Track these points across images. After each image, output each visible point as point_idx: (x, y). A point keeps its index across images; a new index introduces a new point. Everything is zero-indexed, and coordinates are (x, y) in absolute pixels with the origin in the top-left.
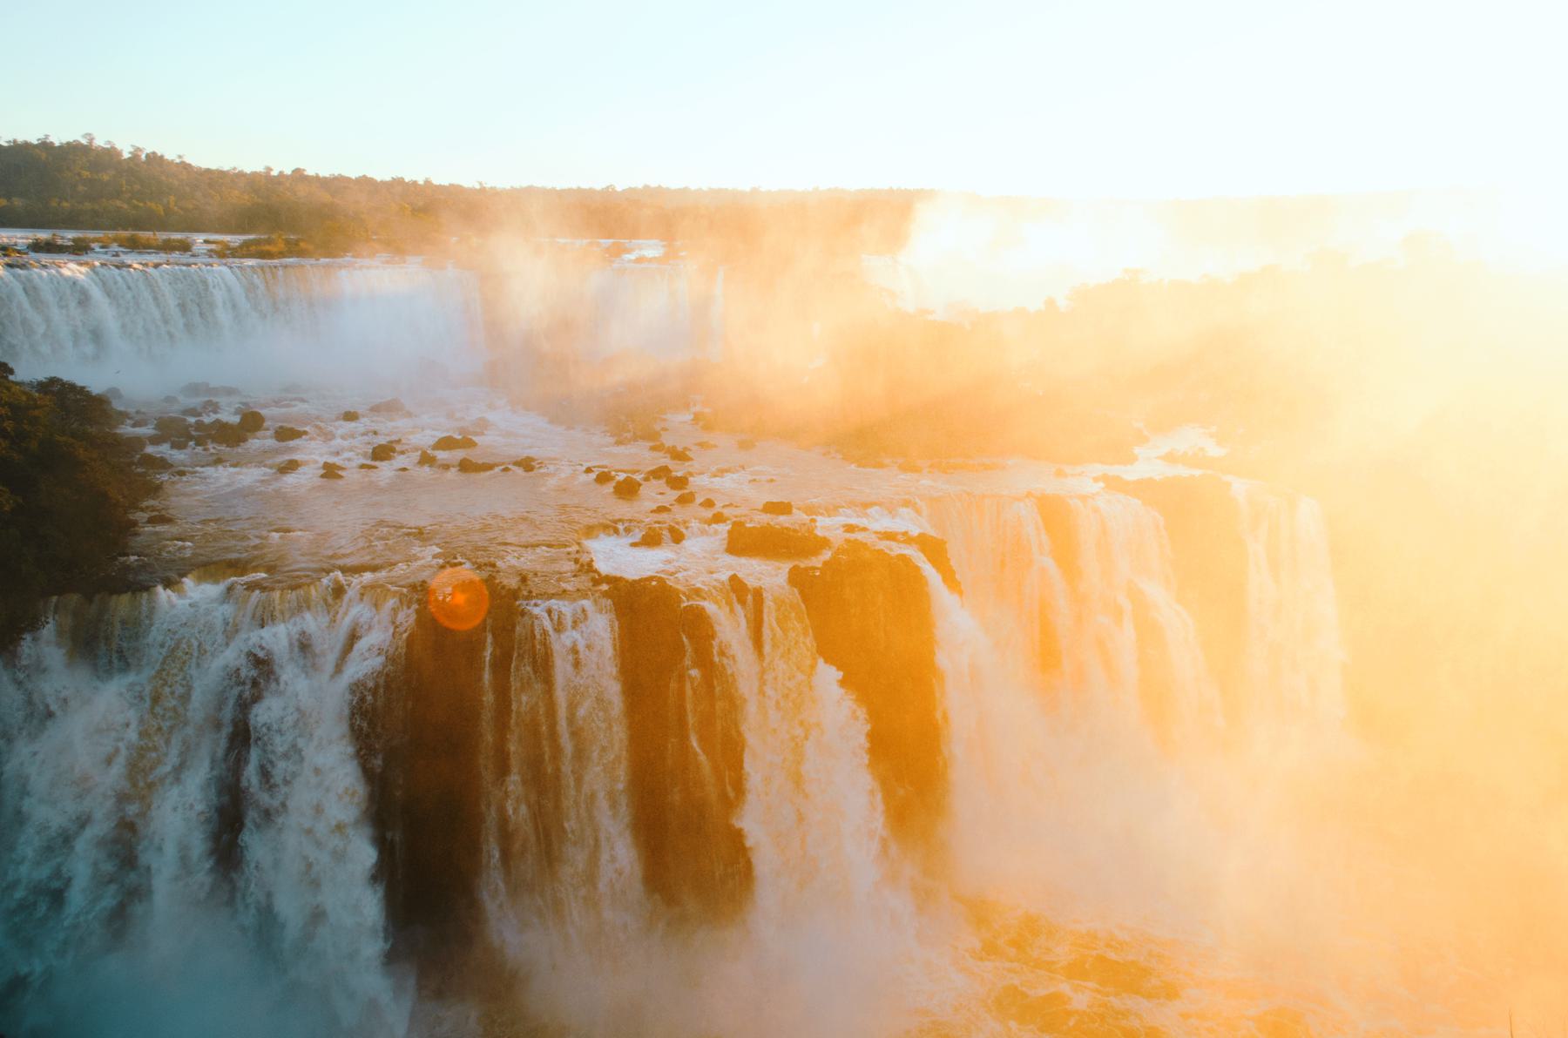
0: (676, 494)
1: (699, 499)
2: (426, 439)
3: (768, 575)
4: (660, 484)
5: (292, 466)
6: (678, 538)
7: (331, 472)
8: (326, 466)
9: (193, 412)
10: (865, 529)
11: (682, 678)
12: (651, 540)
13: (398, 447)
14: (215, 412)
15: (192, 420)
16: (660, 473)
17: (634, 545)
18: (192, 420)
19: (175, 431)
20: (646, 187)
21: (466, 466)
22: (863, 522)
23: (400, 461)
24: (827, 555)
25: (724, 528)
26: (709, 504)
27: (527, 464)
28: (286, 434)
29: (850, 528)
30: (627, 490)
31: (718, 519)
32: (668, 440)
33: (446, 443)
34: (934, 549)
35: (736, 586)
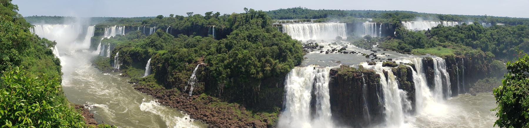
2: (339, 49)
3: (388, 69)
4: (372, 56)
5: (321, 52)
6: (375, 64)
7: (327, 53)
12: (370, 64)
16: (372, 54)
21: (345, 53)
23: (335, 51)
25: (382, 62)
26: (380, 59)
27: (353, 52)
28: (322, 47)
30: (368, 57)
31: (381, 61)
32: (373, 49)
33: (341, 49)
34: (413, 66)
35: (384, 71)
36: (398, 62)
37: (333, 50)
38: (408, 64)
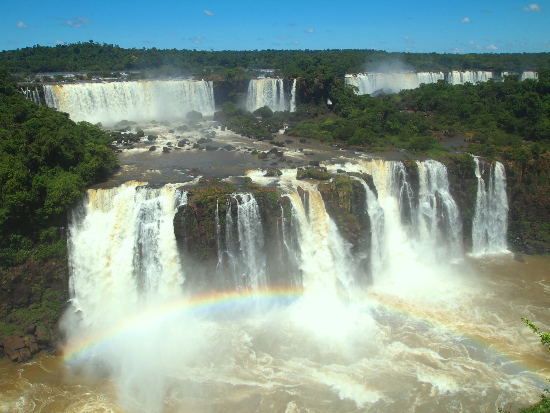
0: (278, 158)
1: (287, 160)
8: (164, 148)
9: (124, 131)
10: (344, 172)
11: (280, 221)
13: (187, 142)
14: (130, 130)
15: (123, 133)
17: (265, 176)
18: (123, 133)
19: (118, 136)
20: (268, 50)
22: (343, 169)
23: (187, 146)
24: (331, 180)
25: (296, 170)
29: (339, 171)
31: (293, 167)
32: (275, 139)
33: (202, 141)
34: (369, 179)
36: (333, 168)
37: (182, 144)
38: (357, 174)
